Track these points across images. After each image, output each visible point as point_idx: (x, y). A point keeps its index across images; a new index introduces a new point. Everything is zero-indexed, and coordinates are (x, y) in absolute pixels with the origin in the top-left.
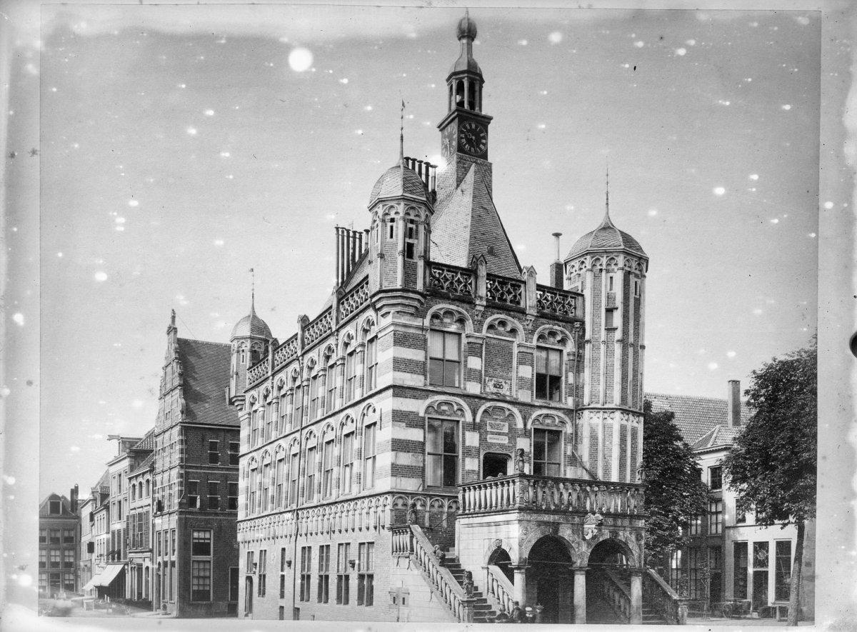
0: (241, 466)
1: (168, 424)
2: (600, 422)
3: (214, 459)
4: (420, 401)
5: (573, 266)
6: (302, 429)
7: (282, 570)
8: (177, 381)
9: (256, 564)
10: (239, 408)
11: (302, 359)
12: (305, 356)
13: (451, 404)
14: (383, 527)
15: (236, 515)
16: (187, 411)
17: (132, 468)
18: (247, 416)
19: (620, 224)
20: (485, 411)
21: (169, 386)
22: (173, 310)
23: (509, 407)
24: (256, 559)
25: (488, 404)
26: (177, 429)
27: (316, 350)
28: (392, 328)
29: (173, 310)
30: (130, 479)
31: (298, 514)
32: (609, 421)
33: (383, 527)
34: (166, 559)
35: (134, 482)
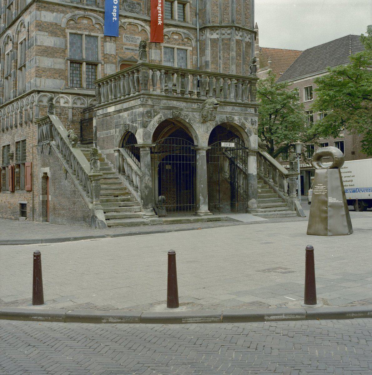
4: (62, 15)
13: (89, 18)
14: (32, 122)
33: (32, 122)
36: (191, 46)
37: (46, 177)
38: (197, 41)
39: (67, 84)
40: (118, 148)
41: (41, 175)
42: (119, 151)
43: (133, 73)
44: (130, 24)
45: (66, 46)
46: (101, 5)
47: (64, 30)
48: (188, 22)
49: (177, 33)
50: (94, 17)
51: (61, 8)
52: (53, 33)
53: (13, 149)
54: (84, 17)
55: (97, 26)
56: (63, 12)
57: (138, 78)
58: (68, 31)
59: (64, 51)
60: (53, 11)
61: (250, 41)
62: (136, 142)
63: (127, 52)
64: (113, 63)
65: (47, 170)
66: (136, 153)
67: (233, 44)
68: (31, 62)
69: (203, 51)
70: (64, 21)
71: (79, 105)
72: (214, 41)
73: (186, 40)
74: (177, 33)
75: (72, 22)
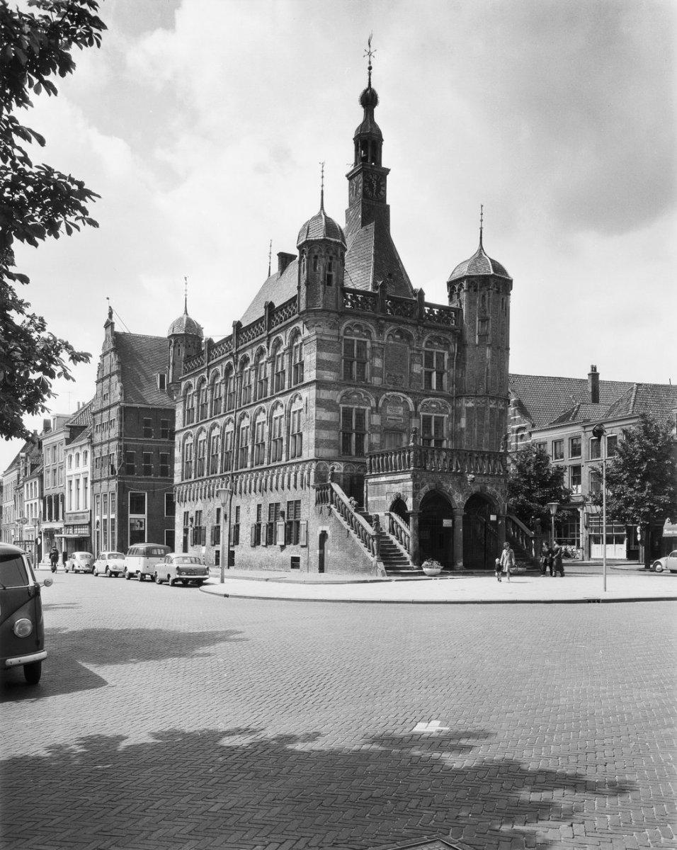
0: (176, 440)
1: (106, 404)
3: (148, 434)
4: (337, 392)
7: (218, 522)
8: (115, 368)
9: (192, 519)
14: (309, 485)
15: (172, 481)
19: (492, 252)
20: (385, 399)
21: (107, 372)
22: (110, 307)
23: (405, 396)
24: (192, 514)
25: (387, 394)
26: (114, 411)
29: (110, 307)
30: (66, 450)
33: (309, 485)
34: (105, 517)
35: (70, 452)
36: (447, 413)
37: (323, 536)
38: (453, 409)
39: (339, 453)
40: (388, 512)
41: (319, 533)
42: (390, 515)
43: (404, 452)
44: (393, 396)
45: (340, 419)
46: (369, 381)
47: (337, 406)
48: (445, 391)
49: (434, 403)
50: (363, 392)
52: (329, 409)
53: (283, 507)
54: (355, 393)
55: (366, 400)
56: (337, 389)
57: (409, 457)
58: (341, 406)
59: (338, 423)
60: (329, 389)
61: (503, 408)
62: (406, 509)
63: (391, 422)
64: (377, 433)
65: (326, 528)
66: (405, 518)
67: (488, 414)
69: (458, 419)
70: (339, 397)
71: (349, 471)
72: (469, 409)
73: (443, 408)
74: (434, 403)
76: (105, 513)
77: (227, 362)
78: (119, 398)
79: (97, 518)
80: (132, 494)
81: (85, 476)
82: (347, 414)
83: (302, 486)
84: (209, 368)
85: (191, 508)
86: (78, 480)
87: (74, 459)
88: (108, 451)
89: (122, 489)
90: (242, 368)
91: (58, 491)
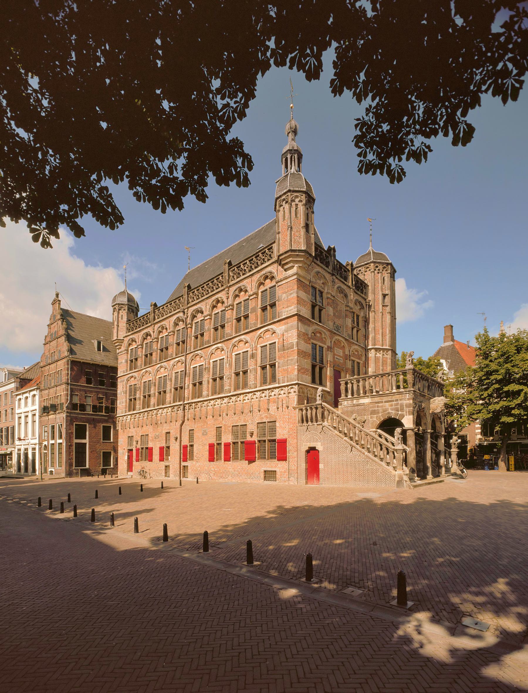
2: (381, 355)
5: (360, 270)
6: (186, 354)
10: (117, 347)
11: (187, 311)
12: (190, 309)
16: (71, 351)
17: (17, 389)
18: (126, 352)
27: (203, 303)
28: (295, 277)
31: (184, 407)
32: (386, 356)
34: (53, 442)
51: (309, 323)
56: (309, 326)
68: (289, 361)
75: (313, 334)
76: (53, 438)
77: (175, 317)
78: (66, 354)
79: (46, 443)
80: (75, 424)
81: (33, 413)
82: (314, 346)
83: (278, 408)
84: (155, 324)
85: (136, 433)
86: (27, 416)
87: (23, 401)
88: (56, 394)
89: (70, 420)
90: (192, 321)
91: (10, 425)
